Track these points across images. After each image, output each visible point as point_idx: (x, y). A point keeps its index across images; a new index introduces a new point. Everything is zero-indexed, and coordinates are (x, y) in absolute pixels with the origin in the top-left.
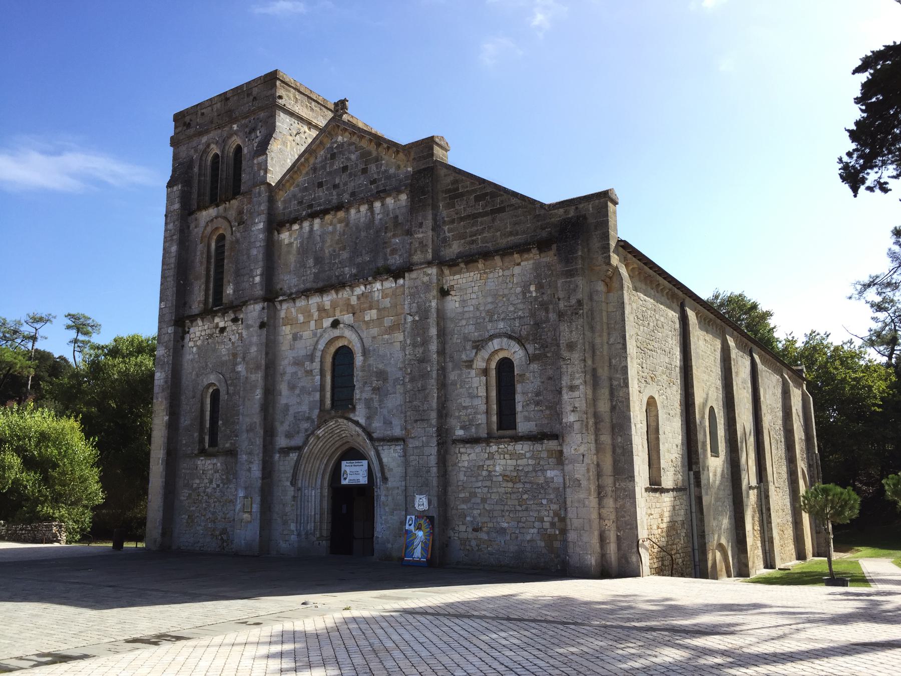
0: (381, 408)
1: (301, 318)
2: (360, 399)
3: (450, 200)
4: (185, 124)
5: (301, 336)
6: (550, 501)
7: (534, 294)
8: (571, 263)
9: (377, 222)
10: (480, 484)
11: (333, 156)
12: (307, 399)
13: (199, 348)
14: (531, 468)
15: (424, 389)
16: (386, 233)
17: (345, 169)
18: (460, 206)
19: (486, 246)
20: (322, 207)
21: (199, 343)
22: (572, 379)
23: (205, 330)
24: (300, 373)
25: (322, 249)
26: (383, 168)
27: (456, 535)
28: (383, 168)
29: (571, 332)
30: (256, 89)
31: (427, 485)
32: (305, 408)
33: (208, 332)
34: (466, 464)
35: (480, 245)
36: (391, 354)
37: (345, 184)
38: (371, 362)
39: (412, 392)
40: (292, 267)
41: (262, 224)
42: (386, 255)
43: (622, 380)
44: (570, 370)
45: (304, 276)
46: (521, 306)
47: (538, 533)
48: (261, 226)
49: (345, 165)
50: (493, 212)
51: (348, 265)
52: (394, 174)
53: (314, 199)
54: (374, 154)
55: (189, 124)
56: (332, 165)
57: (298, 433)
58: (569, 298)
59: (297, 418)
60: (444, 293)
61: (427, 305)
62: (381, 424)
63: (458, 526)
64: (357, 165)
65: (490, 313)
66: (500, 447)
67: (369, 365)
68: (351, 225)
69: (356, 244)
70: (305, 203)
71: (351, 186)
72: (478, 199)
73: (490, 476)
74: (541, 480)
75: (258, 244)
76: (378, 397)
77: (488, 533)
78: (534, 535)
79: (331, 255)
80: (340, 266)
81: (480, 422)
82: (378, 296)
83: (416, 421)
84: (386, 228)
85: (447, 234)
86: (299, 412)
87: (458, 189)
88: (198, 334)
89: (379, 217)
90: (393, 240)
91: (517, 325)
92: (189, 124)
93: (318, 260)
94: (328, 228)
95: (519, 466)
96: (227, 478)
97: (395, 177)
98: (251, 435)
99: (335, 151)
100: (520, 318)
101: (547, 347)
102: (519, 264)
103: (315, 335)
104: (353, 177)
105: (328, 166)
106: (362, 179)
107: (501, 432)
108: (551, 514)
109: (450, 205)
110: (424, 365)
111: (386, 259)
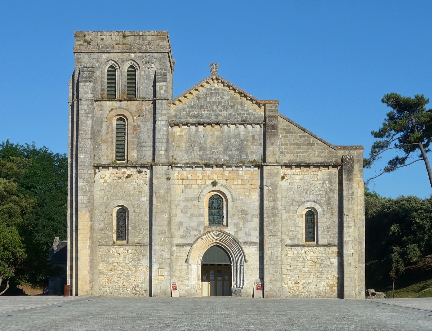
0: (244, 228)
1: (190, 177)
2: (231, 223)
3: (285, 134)
4: (85, 41)
5: (190, 187)
6: (332, 271)
7: (328, 185)
8: (350, 176)
9: (241, 136)
10: (299, 264)
11: (211, 93)
13: (109, 184)
15: (274, 221)
16: (247, 142)
17: (220, 103)
18: (292, 138)
19: (304, 160)
20: (204, 120)
21: (108, 181)
23: (114, 174)
25: (205, 142)
26: (245, 109)
27: (286, 285)
28: (245, 109)
29: (349, 204)
31: (276, 264)
32: (194, 224)
33: (118, 175)
34: (292, 255)
35: (302, 159)
36: (250, 203)
37: (220, 111)
38: (238, 205)
39: (268, 222)
40: (184, 148)
41: (165, 122)
42: (247, 153)
43: (362, 225)
44: (348, 220)
45: (192, 155)
46: (322, 189)
47: (326, 284)
48: (164, 122)
49: (219, 100)
50: (308, 144)
51: (223, 154)
52: (253, 113)
53: (198, 114)
54: (240, 100)
55: (90, 42)
56: (211, 98)
57: (190, 236)
58: (349, 190)
59: (189, 229)
60: (283, 178)
61: (276, 183)
62: (244, 235)
63: (287, 281)
64: (228, 103)
65: (306, 191)
66: (309, 249)
67: (237, 207)
68: (225, 134)
69: (228, 144)
70: (191, 115)
71: (224, 113)
72: (301, 137)
73: (304, 261)
74: (328, 263)
75: (162, 133)
76: (242, 222)
77: (302, 285)
78: (324, 285)
80: (217, 154)
81: (299, 237)
82: (242, 173)
83: (270, 236)
84: (248, 140)
85: (284, 150)
86: (190, 226)
87: (290, 129)
88: (108, 176)
89: (243, 133)
90: (252, 147)
91: (320, 197)
93: (201, 148)
94: (209, 132)
95: (318, 257)
96: (138, 258)
97: (253, 115)
98: (162, 236)
99: (213, 91)
100: (321, 194)
101: (333, 208)
102: (321, 171)
103: (200, 187)
104: (225, 108)
105: (208, 98)
106: (232, 111)
107: (308, 242)
108: (333, 276)
109: (284, 137)
110: (275, 210)
111: (247, 156)
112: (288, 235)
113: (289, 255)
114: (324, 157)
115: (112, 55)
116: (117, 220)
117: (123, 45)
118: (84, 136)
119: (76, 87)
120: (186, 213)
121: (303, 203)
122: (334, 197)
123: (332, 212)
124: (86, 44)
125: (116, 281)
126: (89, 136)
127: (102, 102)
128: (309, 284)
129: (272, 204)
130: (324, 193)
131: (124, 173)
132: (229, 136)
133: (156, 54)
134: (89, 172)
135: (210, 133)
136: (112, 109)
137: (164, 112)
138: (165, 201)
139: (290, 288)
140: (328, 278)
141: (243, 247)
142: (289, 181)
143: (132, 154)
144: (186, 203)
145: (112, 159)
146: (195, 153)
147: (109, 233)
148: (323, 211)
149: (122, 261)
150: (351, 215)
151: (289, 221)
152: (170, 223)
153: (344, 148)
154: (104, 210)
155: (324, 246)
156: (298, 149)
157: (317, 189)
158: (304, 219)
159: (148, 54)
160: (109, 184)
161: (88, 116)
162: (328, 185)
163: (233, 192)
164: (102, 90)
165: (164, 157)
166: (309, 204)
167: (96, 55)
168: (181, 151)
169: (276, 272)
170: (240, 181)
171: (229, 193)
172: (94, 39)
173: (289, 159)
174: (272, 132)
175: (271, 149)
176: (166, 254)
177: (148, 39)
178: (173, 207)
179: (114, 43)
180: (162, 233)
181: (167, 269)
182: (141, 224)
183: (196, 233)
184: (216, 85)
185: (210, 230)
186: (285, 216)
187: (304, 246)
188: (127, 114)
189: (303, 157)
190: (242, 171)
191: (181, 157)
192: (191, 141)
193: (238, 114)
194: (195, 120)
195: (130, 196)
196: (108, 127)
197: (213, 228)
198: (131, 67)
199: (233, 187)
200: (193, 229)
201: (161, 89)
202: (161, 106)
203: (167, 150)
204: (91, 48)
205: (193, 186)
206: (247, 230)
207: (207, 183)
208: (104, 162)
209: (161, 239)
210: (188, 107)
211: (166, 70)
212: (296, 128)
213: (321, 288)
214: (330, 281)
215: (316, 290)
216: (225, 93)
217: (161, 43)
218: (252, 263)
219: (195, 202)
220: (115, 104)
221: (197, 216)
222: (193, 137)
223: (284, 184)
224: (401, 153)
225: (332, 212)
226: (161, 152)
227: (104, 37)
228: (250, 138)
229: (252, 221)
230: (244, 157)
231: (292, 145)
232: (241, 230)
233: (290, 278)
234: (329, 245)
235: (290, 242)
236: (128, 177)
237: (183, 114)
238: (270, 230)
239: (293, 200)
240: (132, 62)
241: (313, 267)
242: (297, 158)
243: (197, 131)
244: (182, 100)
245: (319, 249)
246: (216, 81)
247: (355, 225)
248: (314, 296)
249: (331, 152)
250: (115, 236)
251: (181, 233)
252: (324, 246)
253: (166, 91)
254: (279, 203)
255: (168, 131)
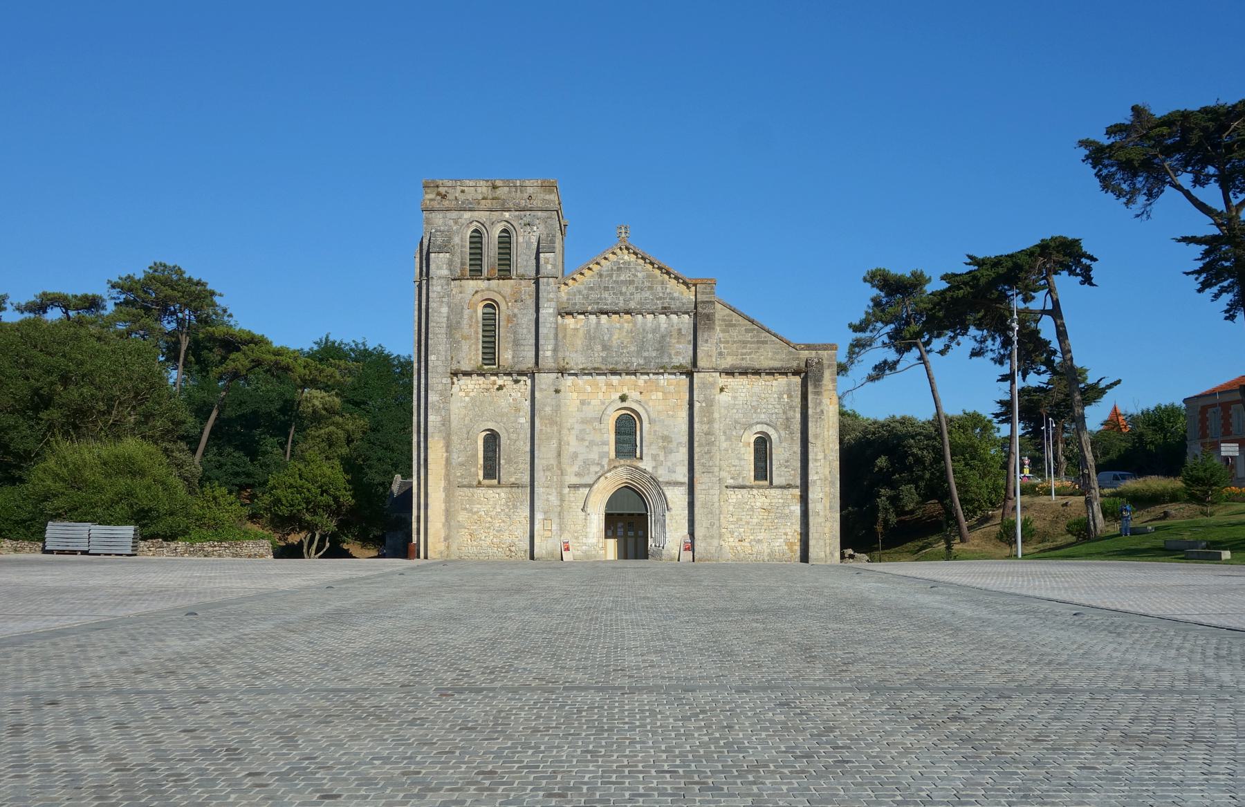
1: (589, 389)
2: (647, 454)
4: (438, 194)
5: (589, 403)
6: (792, 524)
9: (662, 329)
10: (745, 513)
11: (619, 269)
12: (595, 448)
13: (472, 398)
14: (780, 505)
15: (709, 452)
17: (631, 282)
18: (734, 333)
21: (471, 394)
22: (816, 456)
24: (588, 431)
25: (610, 339)
26: (668, 291)
28: (668, 291)
30: (531, 188)
33: (485, 386)
34: (734, 500)
40: (580, 348)
48: (551, 311)
50: (758, 342)
53: (600, 299)
54: (660, 278)
55: (445, 195)
56: (619, 275)
57: (588, 474)
59: (587, 464)
60: (722, 390)
64: (643, 282)
65: (755, 408)
67: (655, 431)
71: (637, 297)
72: (747, 331)
73: (752, 509)
75: (549, 325)
77: (750, 543)
79: (619, 345)
85: (723, 350)
87: (732, 321)
88: (471, 387)
89: (666, 326)
90: (677, 346)
92: (445, 195)
93: (605, 347)
96: (513, 505)
98: (549, 474)
99: (622, 266)
100: (776, 413)
102: (776, 380)
105: (614, 276)
107: (757, 482)
109: (723, 331)
111: (671, 358)
112: (729, 472)
113: (730, 501)
114: (781, 360)
115: (476, 213)
116: (484, 451)
117: (493, 199)
118: (437, 329)
119: (426, 260)
120: (583, 440)
121: (751, 426)
122: (794, 418)
123: (792, 438)
124: (439, 198)
125: (483, 538)
126: (443, 331)
127: (463, 282)
128: (759, 541)
129: (705, 427)
130: (781, 411)
131: (494, 383)
132: (644, 330)
133: (539, 213)
134: (444, 381)
135: (618, 325)
136: (477, 292)
137: (551, 296)
138: (553, 422)
139: (732, 548)
140: (786, 534)
141: (665, 489)
142: (730, 394)
143: (506, 356)
144: (584, 426)
145: (477, 363)
146: (596, 355)
147: (473, 470)
148: (780, 437)
149: (491, 509)
150: (819, 443)
151: (730, 451)
152: (560, 455)
153: (809, 347)
154: (465, 436)
155: (781, 487)
156: (743, 348)
157: (770, 406)
158: (752, 449)
159: (528, 213)
160: (472, 398)
161: (442, 302)
162: (786, 400)
163: (650, 409)
164: (463, 264)
165: (551, 360)
166: (759, 428)
167: (454, 215)
168: (576, 352)
169: (712, 525)
170: (660, 395)
171: (644, 411)
172: (450, 190)
173: (730, 363)
174: (706, 324)
175: (706, 349)
176: (554, 499)
177: (528, 191)
178: (565, 432)
179: (480, 197)
180: (548, 468)
181: (556, 520)
182: (518, 457)
183: (597, 469)
184: (626, 257)
185: (617, 464)
186: (724, 445)
187: (752, 487)
188: (498, 298)
189: (751, 359)
190: (663, 380)
191: (576, 360)
192: (591, 337)
193: (657, 299)
194: (596, 307)
195: (502, 415)
196: (471, 318)
197: (622, 462)
198: (505, 231)
199: (651, 404)
200: (593, 464)
201: (547, 263)
202: (547, 286)
203: (555, 350)
204: (446, 203)
205: (593, 402)
206: (669, 464)
207: (613, 397)
208: (466, 367)
209: (547, 477)
210: (585, 288)
211: (554, 236)
212: (740, 318)
213: (776, 548)
214: (789, 537)
215: (769, 550)
216: (639, 268)
217: (547, 197)
218: (678, 512)
219: (596, 424)
220: (482, 284)
221: (598, 445)
222: (592, 331)
223: (724, 398)
224: (891, 355)
225: (792, 438)
226: (547, 352)
227: (466, 189)
228: (675, 333)
229: (678, 452)
230: (666, 360)
231: (735, 342)
232: (662, 465)
233: (732, 533)
234: (789, 486)
235: (732, 481)
236: (500, 388)
237: (578, 299)
238: (703, 465)
239: (736, 422)
240: (506, 223)
241: (765, 517)
242: (742, 362)
243: (598, 323)
244: (577, 279)
245: (773, 491)
246: (625, 251)
247: (825, 458)
248: (766, 559)
249: (790, 352)
250: (481, 473)
251: (575, 468)
252: (781, 487)
253: (554, 266)
254: (716, 426)
255: (557, 323)
